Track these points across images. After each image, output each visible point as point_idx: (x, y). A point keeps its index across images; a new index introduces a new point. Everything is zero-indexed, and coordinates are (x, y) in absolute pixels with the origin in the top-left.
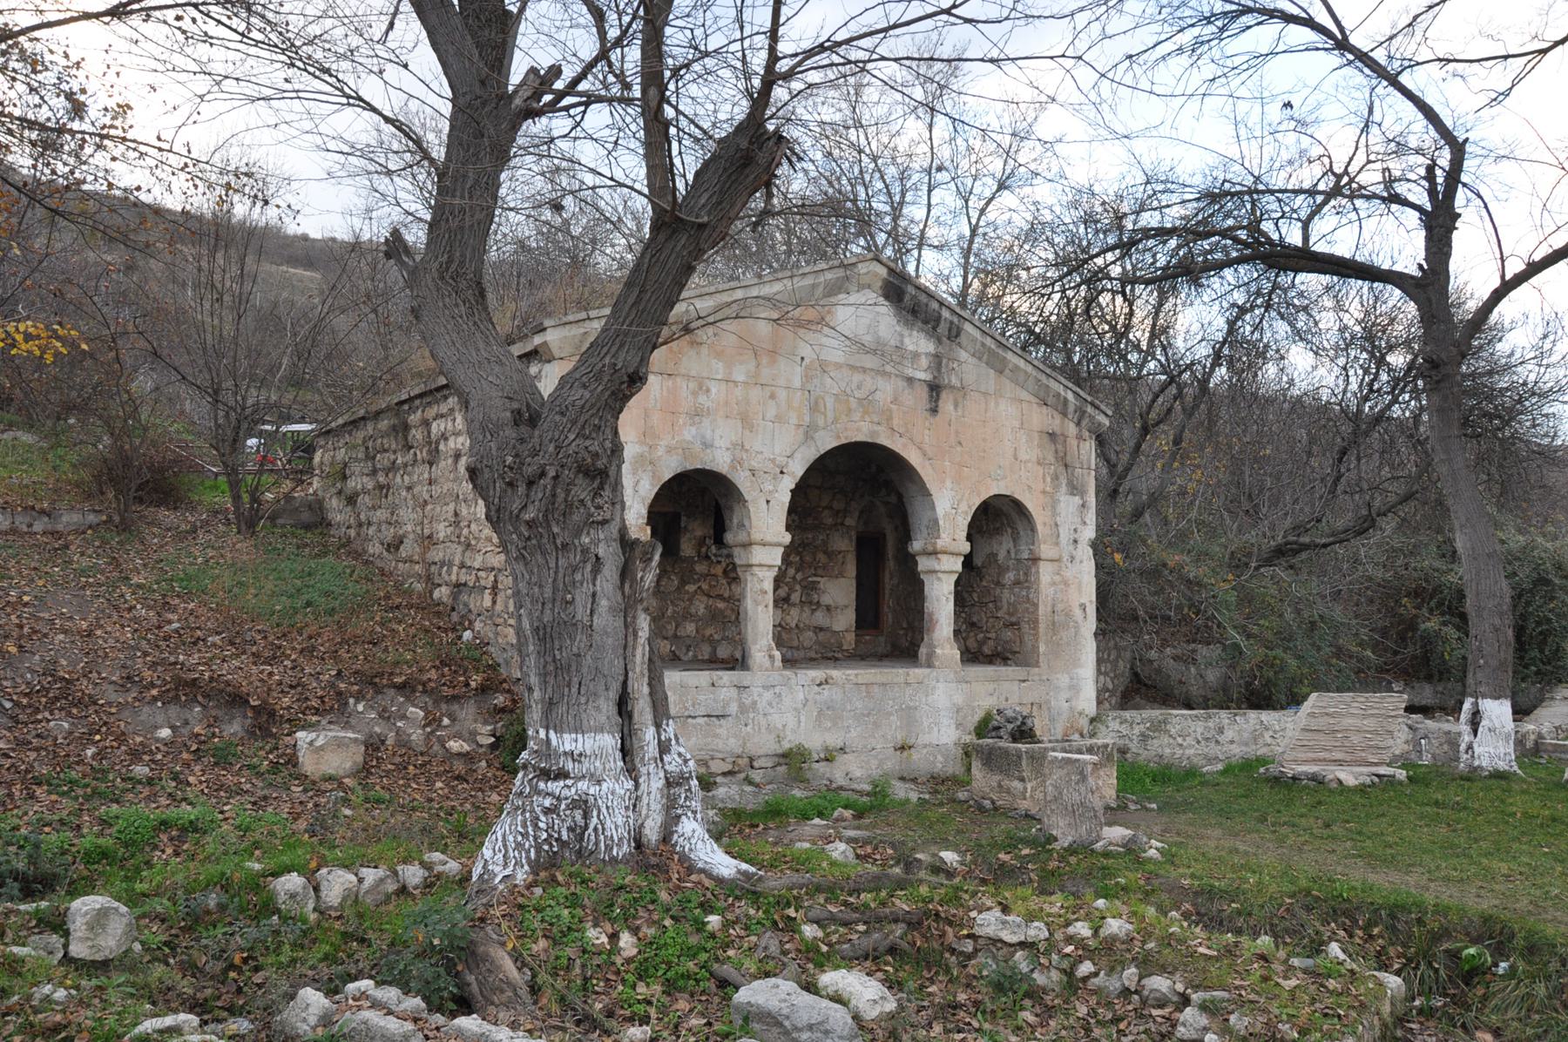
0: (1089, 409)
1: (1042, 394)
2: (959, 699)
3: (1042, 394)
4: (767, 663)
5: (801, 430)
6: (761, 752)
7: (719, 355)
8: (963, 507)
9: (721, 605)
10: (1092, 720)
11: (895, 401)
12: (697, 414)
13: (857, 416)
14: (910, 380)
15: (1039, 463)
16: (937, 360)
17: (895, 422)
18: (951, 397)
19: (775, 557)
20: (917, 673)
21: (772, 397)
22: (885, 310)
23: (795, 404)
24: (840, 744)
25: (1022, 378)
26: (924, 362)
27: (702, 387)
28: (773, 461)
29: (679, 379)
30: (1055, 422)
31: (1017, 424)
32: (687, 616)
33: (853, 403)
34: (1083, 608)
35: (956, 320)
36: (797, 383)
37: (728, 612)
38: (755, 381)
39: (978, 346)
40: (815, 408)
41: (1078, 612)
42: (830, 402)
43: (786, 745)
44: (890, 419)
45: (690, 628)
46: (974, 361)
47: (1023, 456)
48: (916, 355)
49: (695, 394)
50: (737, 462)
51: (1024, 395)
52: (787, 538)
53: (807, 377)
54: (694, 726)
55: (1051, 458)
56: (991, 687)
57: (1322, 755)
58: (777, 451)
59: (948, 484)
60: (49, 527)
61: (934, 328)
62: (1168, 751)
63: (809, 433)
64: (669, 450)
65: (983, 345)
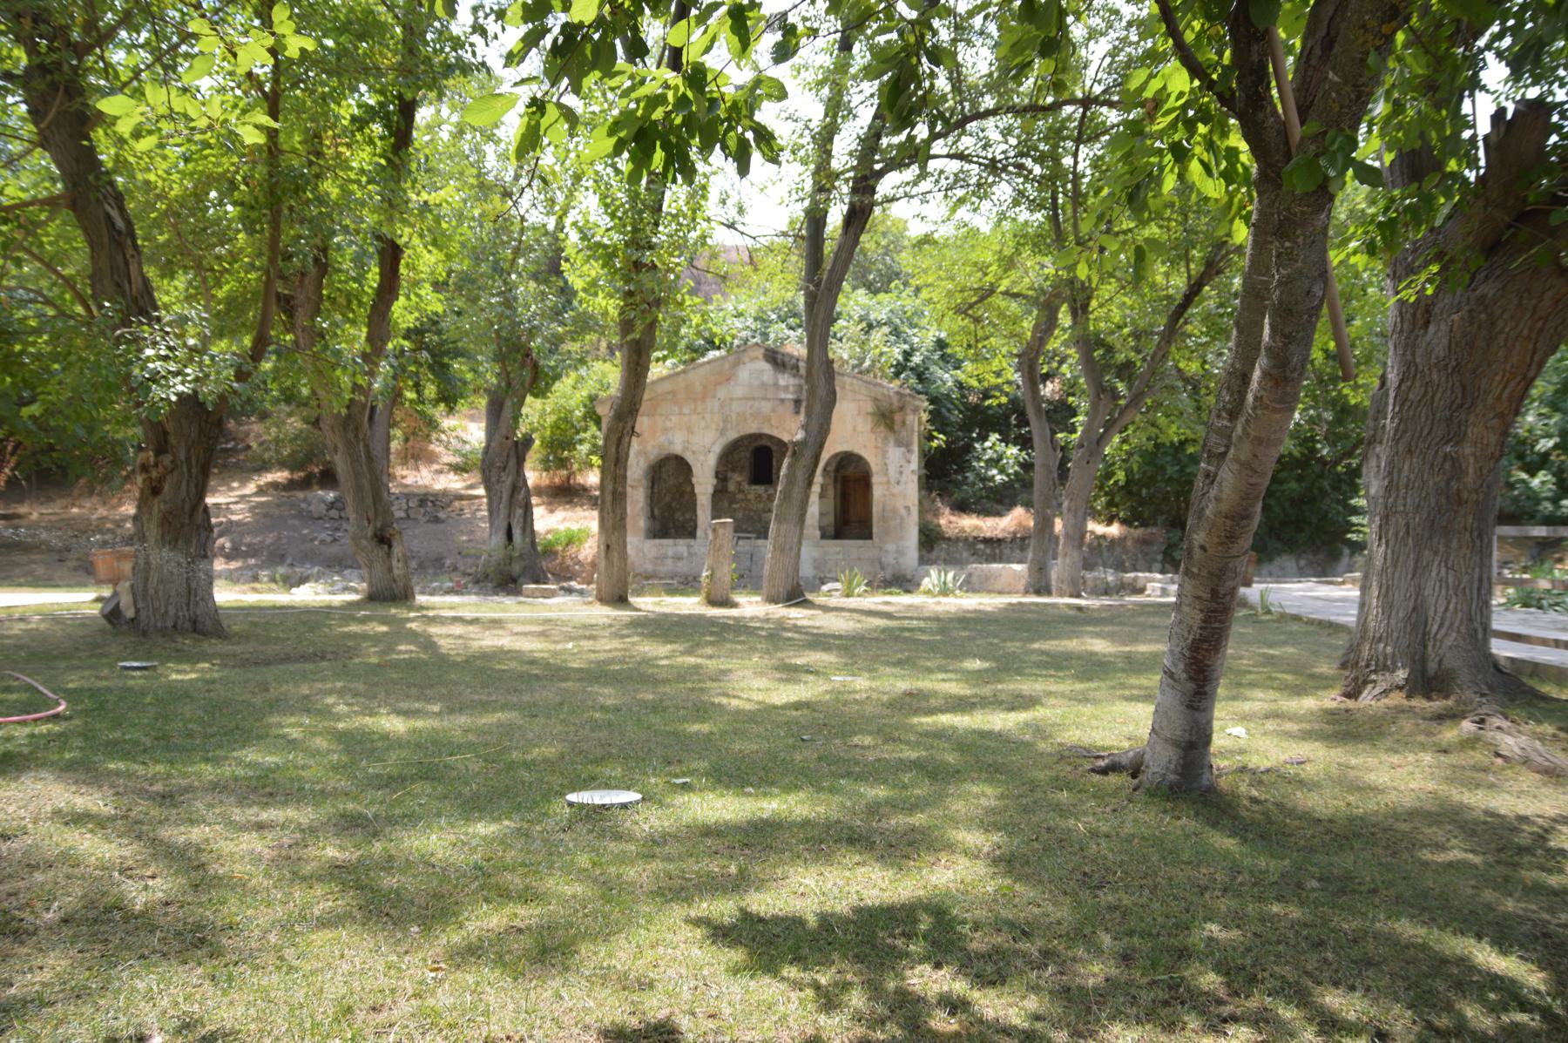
11: (773, 410)
12: (666, 430)
14: (782, 401)
19: (710, 490)
22: (767, 366)
27: (668, 419)
38: (695, 411)
40: (725, 421)
47: (860, 428)
50: (685, 449)
53: (722, 406)
63: (722, 432)
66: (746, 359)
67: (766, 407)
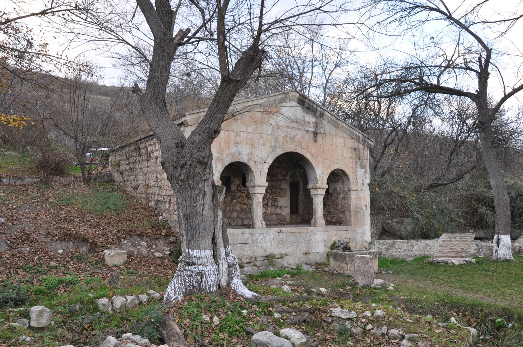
0: (367, 140)
1: (351, 135)
2: (325, 237)
3: (351, 135)
4: (261, 226)
6: (259, 255)
7: (243, 123)
8: (326, 173)
9: (245, 207)
10: (369, 244)
11: (302, 138)
12: (236, 143)
13: (289, 143)
14: (307, 131)
15: (351, 158)
16: (316, 124)
17: (302, 145)
19: (263, 190)
22: (299, 108)
23: (269, 140)
26: (312, 125)
27: (238, 134)
28: (262, 158)
29: (230, 132)
30: (356, 145)
31: (343, 145)
32: (234, 210)
34: (366, 206)
35: (322, 111)
36: (270, 132)
37: (247, 209)
38: (256, 132)
39: (330, 119)
40: (275, 141)
41: (364, 208)
42: (281, 138)
43: (267, 253)
44: (301, 144)
45: (235, 214)
46: (329, 124)
47: (345, 156)
48: (309, 123)
49: (236, 136)
50: (250, 159)
51: (345, 135)
52: (267, 184)
53: (273, 130)
54: (237, 247)
55: (354, 156)
56: (335, 233)
57: (447, 254)
58: (263, 155)
59: (320, 165)
60: (22, 183)
62: (395, 254)
63: (274, 149)
64: (227, 155)
65: (331, 119)
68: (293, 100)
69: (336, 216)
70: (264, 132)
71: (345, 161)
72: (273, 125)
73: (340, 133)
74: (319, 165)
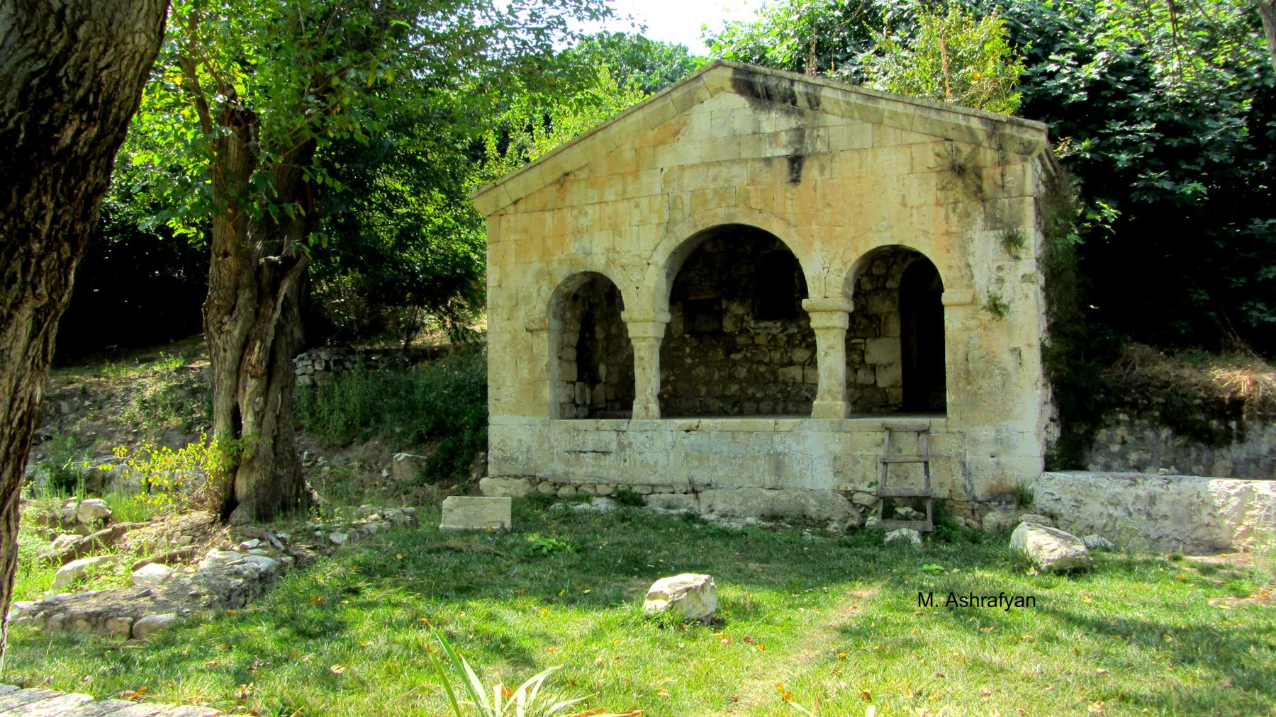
2: (836, 448)
5: (662, 228)
7: (593, 186)
8: (837, 264)
9: (762, 369)
11: (753, 181)
12: (579, 232)
13: (711, 206)
14: (768, 161)
16: (800, 133)
18: (816, 164)
20: (807, 422)
21: (637, 206)
22: (740, 102)
24: (706, 480)
25: (905, 122)
28: (639, 256)
31: (905, 170)
32: (732, 378)
33: (709, 193)
34: (1017, 352)
37: (768, 375)
39: (843, 106)
41: (1008, 360)
42: (686, 198)
45: (734, 388)
46: (845, 121)
47: (913, 200)
48: (775, 135)
50: (609, 262)
53: (666, 182)
61: (794, 103)
63: (669, 227)
64: (561, 262)
65: (848, 103)
66: (704, 94)
67: (740, 175)
68: (722, 89)
69: (918, 383)
70: (644, 193)
71: (914, 219)
72: (665, 170)
73: (891, 136)
74: (811, 244)
